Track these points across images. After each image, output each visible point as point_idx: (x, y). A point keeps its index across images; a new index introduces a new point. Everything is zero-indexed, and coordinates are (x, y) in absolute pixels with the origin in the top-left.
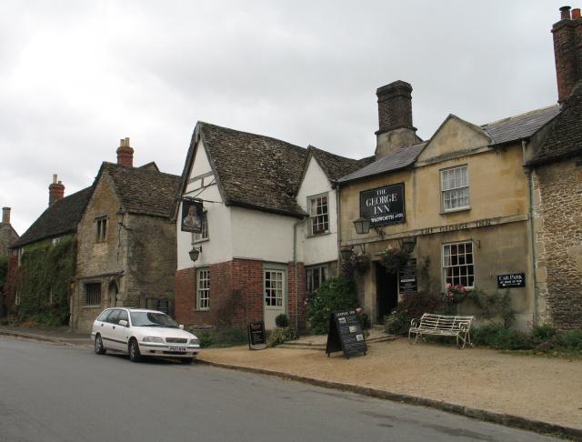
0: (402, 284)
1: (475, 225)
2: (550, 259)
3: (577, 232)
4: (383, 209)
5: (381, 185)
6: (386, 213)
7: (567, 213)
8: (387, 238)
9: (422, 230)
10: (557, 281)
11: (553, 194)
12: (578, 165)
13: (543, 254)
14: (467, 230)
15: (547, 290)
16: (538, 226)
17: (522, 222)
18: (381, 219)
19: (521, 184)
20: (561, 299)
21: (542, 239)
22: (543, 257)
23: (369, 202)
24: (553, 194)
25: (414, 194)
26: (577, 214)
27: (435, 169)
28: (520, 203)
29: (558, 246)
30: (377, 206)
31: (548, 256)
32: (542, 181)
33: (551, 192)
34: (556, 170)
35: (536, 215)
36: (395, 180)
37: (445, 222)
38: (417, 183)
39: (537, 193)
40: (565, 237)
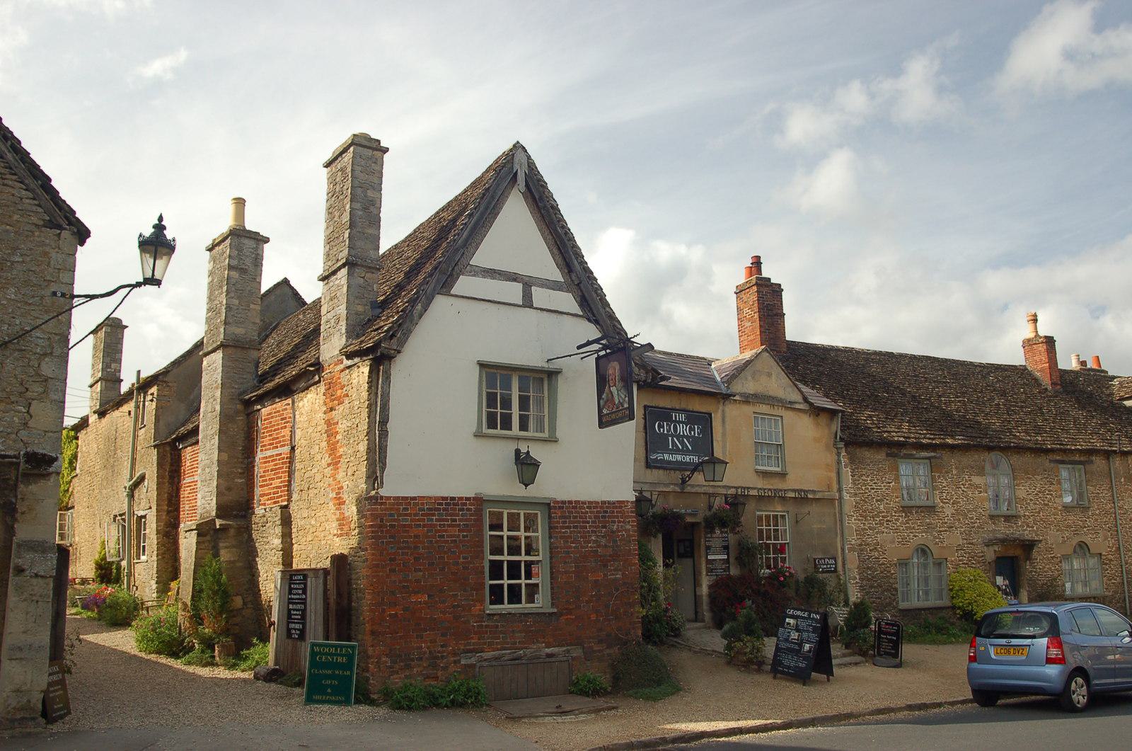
0: (709, 562)
1: (793, 495)
2: (861, 545)
3: (887, 521)
4: (682, 443)
5: (683, 406)
6: (685, 451)
7: (877, 501)
8: (688, 489)
9: (737, 488)
10: (868, 568)
11: (864, 478)
12: (888, 455)
13: (853, 540)
14: (783, 499)
15: (857, 577)
16: (847, 508)
17: (832, 500)
18: (679, 458)
19: (830, 458)
20: (872, 587)
21: (852, 523)
22: (853, 542)
23: (660, 427)
24: (864, 478)
25: (724, 434)
26: (887, 503)
27: (748, 410)
28: (830, 479)
29: (870, 532)
30: (672, 436)
31: (859, 542)
32: (852, 460)
33: (862, 475)
34: (867, 454)
35: (846, 496)
36: (698, 405)
37: (760, 483)
38: (727, 419)
39: (847, 472)
40: (876, 524)
